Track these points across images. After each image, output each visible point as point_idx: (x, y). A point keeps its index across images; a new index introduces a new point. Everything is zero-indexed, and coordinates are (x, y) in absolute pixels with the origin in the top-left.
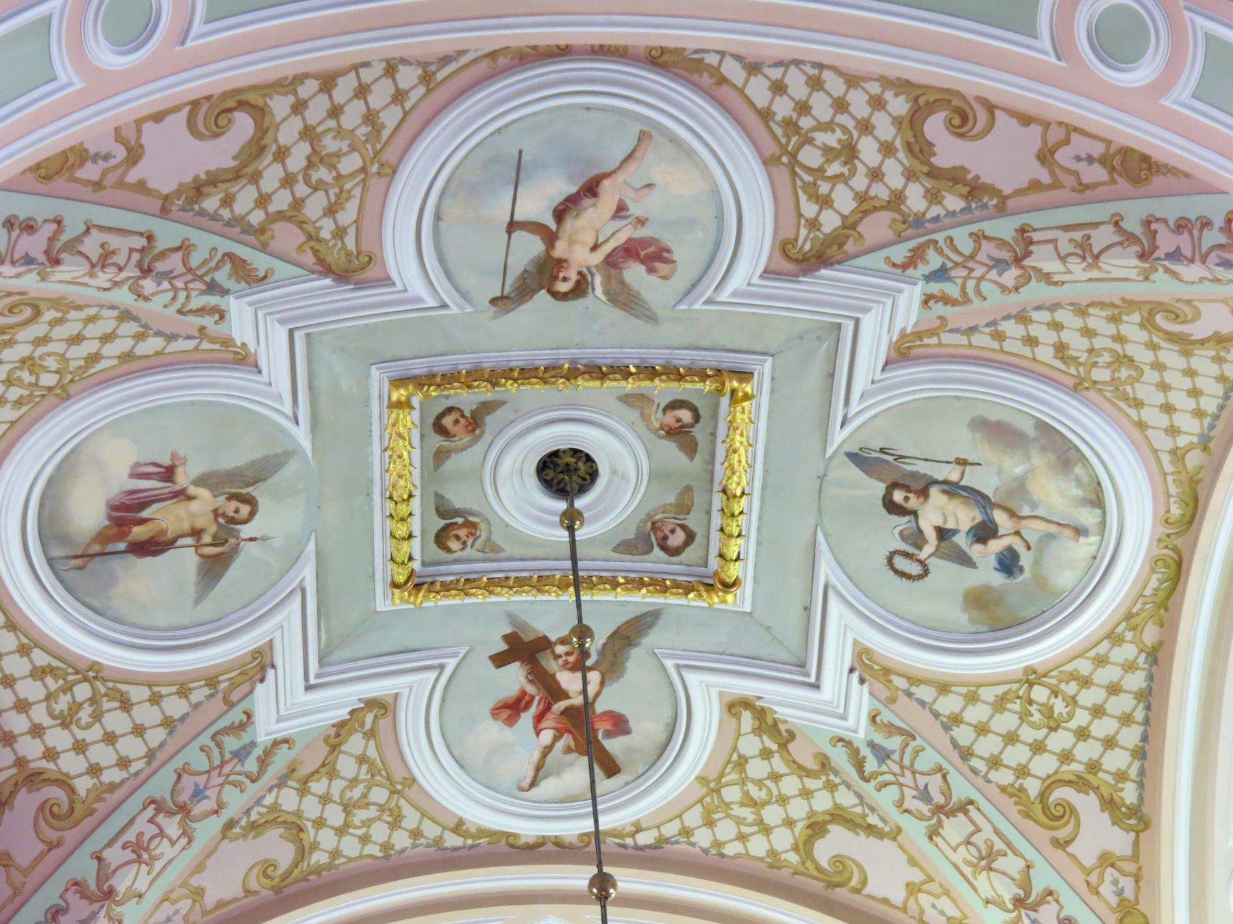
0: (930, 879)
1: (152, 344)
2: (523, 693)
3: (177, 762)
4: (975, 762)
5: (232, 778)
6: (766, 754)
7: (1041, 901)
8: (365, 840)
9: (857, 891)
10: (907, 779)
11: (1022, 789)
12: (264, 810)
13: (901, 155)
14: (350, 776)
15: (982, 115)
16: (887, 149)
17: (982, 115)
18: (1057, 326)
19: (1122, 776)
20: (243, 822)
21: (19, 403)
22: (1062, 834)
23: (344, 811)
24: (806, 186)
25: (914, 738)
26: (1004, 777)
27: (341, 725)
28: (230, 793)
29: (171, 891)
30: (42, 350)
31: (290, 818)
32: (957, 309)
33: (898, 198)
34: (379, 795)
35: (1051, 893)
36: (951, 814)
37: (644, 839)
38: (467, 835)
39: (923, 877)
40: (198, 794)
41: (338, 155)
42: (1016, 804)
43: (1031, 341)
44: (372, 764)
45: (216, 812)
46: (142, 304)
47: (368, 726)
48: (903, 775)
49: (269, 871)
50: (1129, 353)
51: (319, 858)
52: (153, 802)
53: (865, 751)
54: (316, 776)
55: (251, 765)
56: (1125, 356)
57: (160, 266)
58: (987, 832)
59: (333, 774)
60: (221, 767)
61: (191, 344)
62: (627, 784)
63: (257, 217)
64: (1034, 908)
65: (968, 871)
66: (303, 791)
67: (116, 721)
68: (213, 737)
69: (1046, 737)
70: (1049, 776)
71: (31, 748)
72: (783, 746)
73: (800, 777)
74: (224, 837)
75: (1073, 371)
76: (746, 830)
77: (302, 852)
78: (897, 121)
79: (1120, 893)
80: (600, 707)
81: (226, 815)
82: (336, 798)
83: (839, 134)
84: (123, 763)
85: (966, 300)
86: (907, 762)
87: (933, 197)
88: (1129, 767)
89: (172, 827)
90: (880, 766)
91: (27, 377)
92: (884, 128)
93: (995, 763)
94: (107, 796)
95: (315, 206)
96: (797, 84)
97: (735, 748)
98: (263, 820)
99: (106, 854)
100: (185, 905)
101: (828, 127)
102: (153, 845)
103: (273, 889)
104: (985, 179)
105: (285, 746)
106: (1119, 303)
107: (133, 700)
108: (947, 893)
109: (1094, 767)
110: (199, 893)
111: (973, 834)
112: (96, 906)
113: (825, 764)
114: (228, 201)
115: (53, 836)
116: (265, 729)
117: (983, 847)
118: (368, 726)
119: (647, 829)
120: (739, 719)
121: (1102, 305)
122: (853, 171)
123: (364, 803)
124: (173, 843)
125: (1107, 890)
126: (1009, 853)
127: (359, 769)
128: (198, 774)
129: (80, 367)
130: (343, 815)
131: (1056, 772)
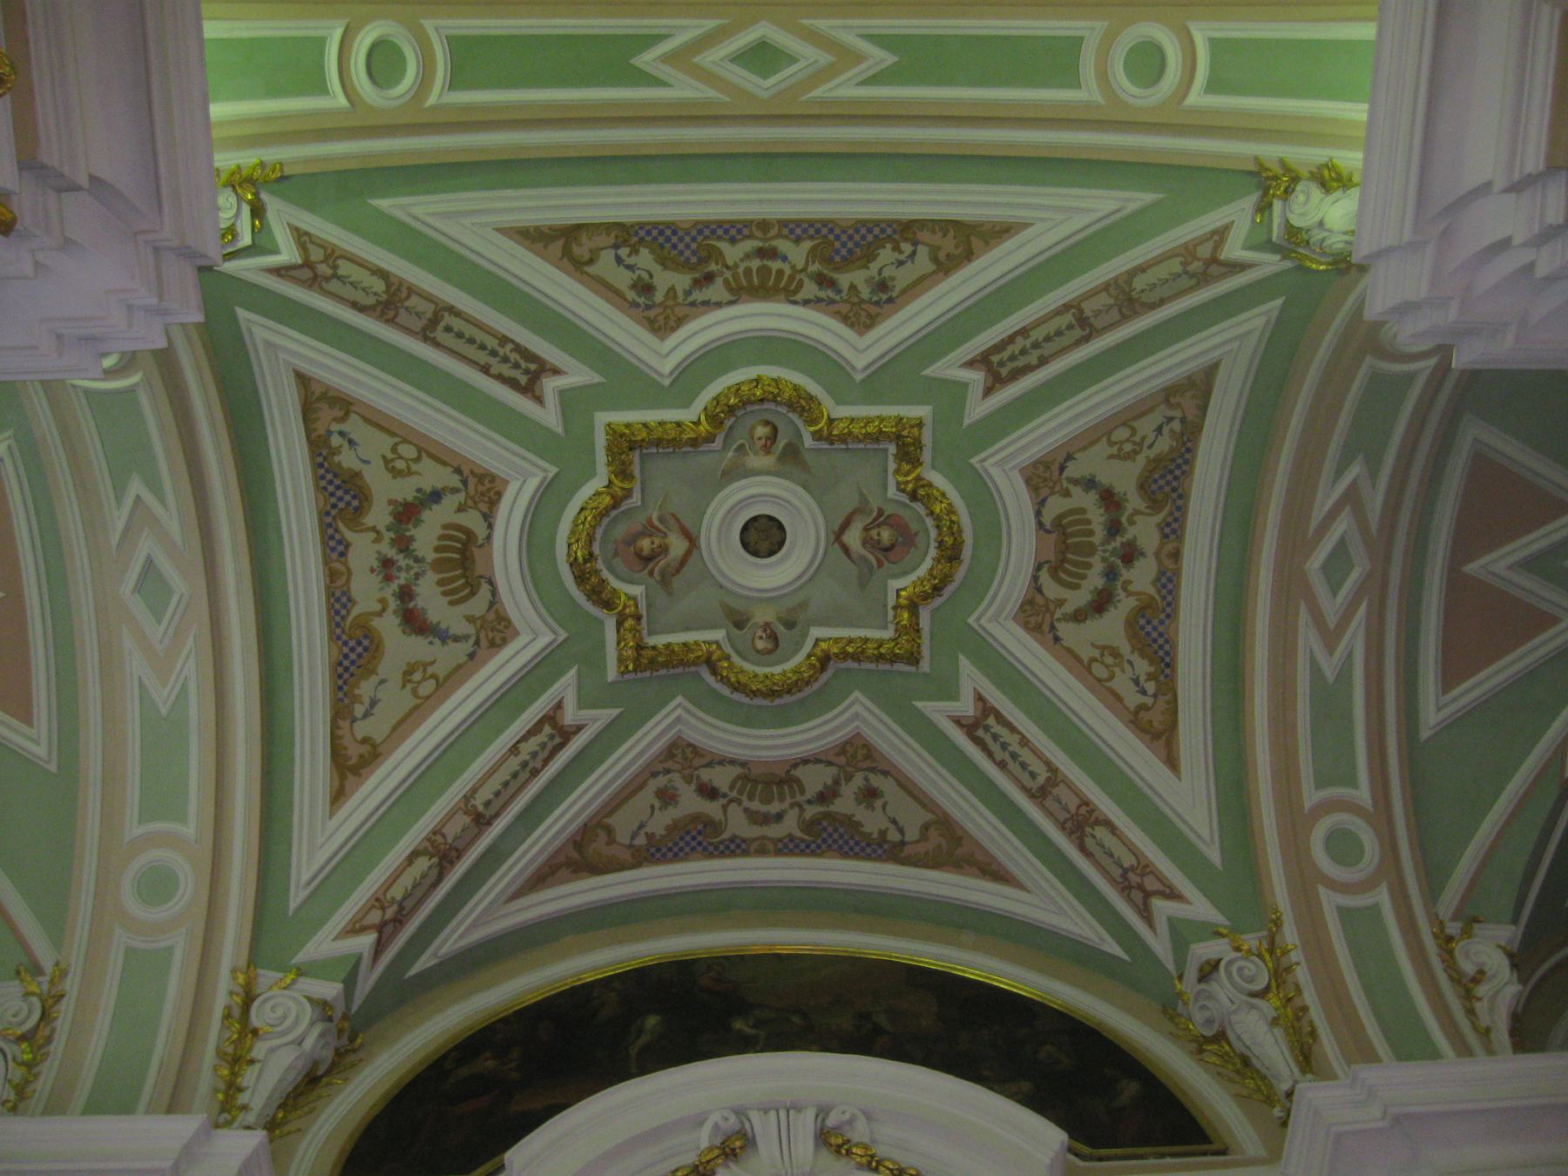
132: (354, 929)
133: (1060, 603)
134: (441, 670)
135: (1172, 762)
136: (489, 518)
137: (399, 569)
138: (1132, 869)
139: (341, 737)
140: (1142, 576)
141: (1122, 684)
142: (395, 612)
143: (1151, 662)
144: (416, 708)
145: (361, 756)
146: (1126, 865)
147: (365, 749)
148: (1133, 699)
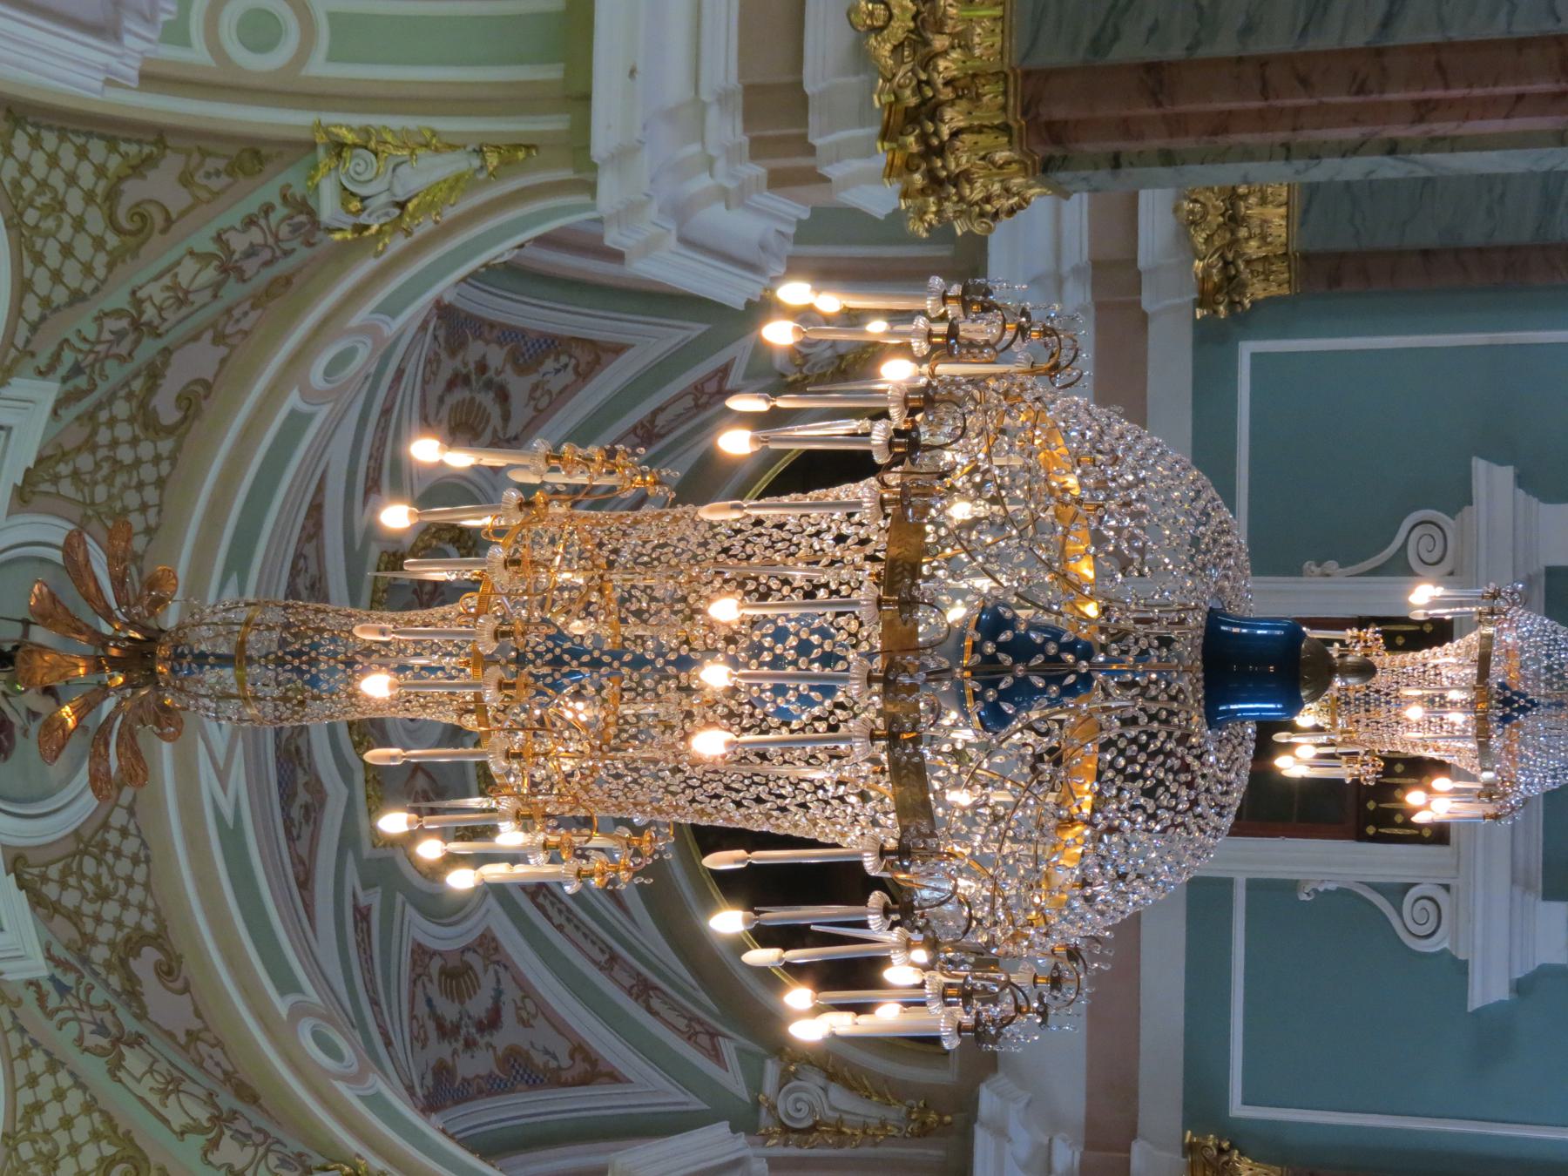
1: (33, 310)
13: (120, 936)
15: (179, 985)
16: (118, 923)
17: (179, 985)
18: (60, 1095)
21: (17, 185)
24: (68, 867)
30: (67, 221)
32: (37, 1012)
33: (92, 940)
41: (111, 485)
43: (33, 1081)
46: (95, 313)
50: (62, 1164)
56: (56, 1162)
57: (131, 337)
61: (20, 342)
63: (103, 416)
75: (19, 1126)
78: (138, 927)
83: (112, 885)
85: (50, 1015)
87: (108, 965)
91: (46, 199)
92: (131, 917)
95: (85, 462)
96: (131, 846)
101: (114, 877)
104: (145, 999)
106: (120, 1131)
114: (130, 396)
121: (108, 1118)
122: (91, 901)
129: (33, 246)
132: (716, 1055)
133: (495, 431)
134: (518, 994)
135: (618, 349)
136: (434, 953)
137: (468, 1033)
138: (696, 399)
139: (573, 1078)
140: (496, 357)
141: (556, 383)
142: (492, 1035)
143: (547, 356)
144: (543, 1014)
145: (584, 1060)
146: (693, 404)
147: (578, 1057)
148: (568, 377)
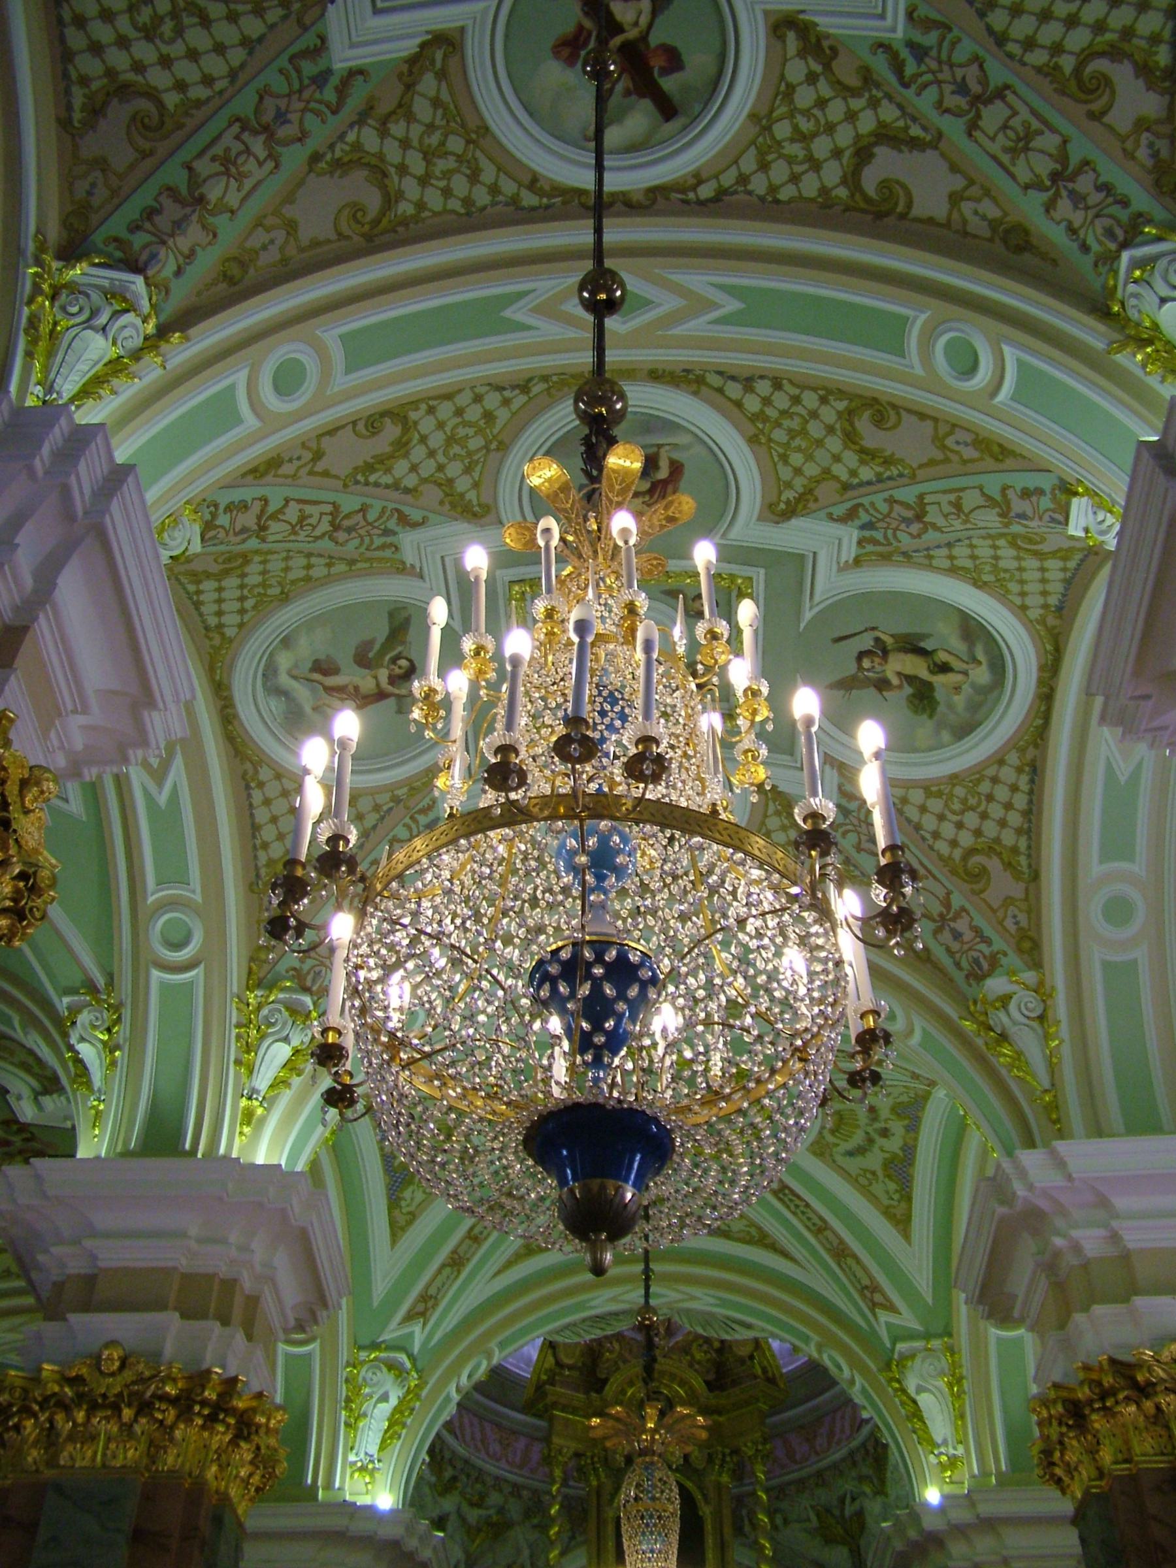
0: (971, 182)
2: (580, 28)
3: (258, 84)
4: (1012, 47)
5: (313, 105)
6: (812, 78)
7: (1078, 172)
8: (447, 192)
9: (903, 217)
10: (946, 75)
11: (1057, 67)
12: (347, 148)
14: (428, 120)
19: (1155, 39)
20: (329, 157)
22: (1096, 107)
23: (425, 158)
25: (950, 29)
26: (1038, 57)
27: (413, 61)
28: (311, 121)
29: (265, 217)
31: (374, 161)
34: (456, 144)
35: (1086, 163)
36: (989, 101)
37: (706, 191)
38: (541, 193)
39: (964, 183)
40: (281, 117)
42: (1052, 82)
44: (445, 109)
45: (300, 140)
47: (438, 65)
48: (941, 71)
49: (359, 214)
51: (405, 208)
52: (238, 119)
53: (905, 53)
54: (394, 117)
55: (330, 95)
58: (1024, 113)
59: (410, 117)
60: (300, 91)
62: (685, 127)
64: (1072, 179)
65: (1005, 159)
66: (384, 133)
67: (197, 37)
68: (292, 59)
69: (1080, 9)
70: (1083, 50)
71: (119, 60)
72: (827, 67)
73: (845, 99)
74: (311, 171)
76: (798, 169)
77: (390, 199)
79: (1155, 155)
80: (654, 40)
81: (311, 145)
82: (415, 143)
84: (208, 81)
86: (944, 56)
88: (1163, 29)
89: (258, 146)
90: (919, 66)
93: (1030, 44)
94: (194, 112)
97: (782, 77)
98: (346, 159)
99: (195, 165)
100: (280, 235)
102: (240, 161)
103: (369, 238)
105: (360, 78)
107: (212, 16)
108: (987, 193)
109: (1127, 33)
110: (291, 227)
111: (1010, 118)
112: (188, 210)
113: (868, 78)
115: (147, 146)
116: (342, 58)
117: (1020, 129)
118: (438, 65)
119: (708, 180)
120: (784, 42)
123: (441, 151)
124: (261, 164)
125: (1142, 154)
126: (1047, 132)
127: (434, 114)
128: (278, 96)
130: (424, 164)
131: (1091, 45)
